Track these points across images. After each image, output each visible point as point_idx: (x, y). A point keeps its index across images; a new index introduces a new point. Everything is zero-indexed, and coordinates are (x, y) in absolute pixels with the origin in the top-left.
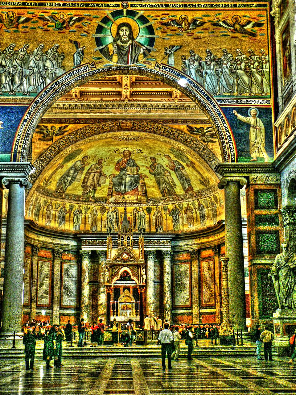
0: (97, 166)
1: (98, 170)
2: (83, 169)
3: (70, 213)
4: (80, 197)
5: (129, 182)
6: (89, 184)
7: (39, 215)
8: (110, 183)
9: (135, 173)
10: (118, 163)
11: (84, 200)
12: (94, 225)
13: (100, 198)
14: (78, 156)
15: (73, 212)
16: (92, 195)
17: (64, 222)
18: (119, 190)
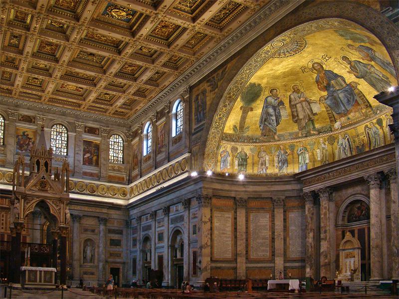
0: (296, 95)
1: (301, 99)
2: (281, 103)
3: (292, 154)
4: (298, 134)
5: (344, 97)
6: (301, 117)
7: (247, 164)
8: (326, 108)
9: (344, 85)
10: (317, 82)
11: (304, 135)
12: (325, 160)
13: (322, 127)
14: (262, 93)
15: (295, 152)
16: (311, 127)
17: (286, 165)
18: (340, 111)
